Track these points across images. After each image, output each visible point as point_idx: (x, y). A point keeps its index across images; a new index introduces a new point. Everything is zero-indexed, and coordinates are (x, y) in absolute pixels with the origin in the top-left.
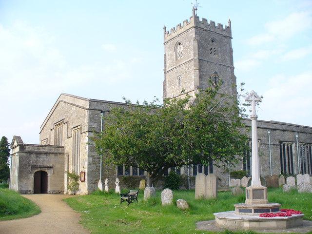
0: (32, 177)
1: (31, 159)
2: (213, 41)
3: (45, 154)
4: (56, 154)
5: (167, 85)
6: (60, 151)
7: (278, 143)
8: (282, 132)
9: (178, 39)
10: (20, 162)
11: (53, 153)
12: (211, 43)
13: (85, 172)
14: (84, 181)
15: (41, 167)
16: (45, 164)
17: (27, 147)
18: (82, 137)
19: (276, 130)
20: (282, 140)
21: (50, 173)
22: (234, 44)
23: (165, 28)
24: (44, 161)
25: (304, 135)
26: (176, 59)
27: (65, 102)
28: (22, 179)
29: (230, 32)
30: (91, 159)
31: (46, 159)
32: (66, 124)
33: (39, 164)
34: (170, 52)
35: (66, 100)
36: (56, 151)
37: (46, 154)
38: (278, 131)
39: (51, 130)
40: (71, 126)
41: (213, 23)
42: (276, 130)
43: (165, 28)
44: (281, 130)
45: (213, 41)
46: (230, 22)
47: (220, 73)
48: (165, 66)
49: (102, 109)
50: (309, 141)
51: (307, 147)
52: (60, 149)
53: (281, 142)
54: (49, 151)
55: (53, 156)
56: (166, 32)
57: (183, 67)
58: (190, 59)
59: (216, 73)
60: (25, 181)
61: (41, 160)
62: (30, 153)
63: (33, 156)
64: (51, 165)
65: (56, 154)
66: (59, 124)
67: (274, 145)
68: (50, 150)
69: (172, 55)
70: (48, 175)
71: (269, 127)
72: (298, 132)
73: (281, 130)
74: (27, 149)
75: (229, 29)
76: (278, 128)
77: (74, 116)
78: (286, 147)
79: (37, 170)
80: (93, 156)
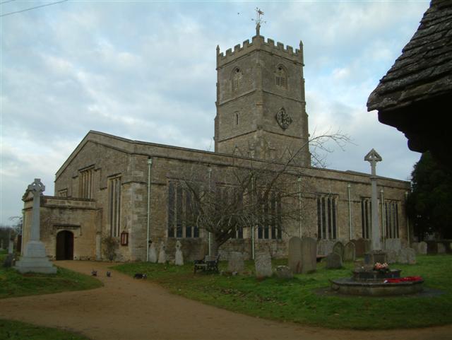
2: (280, 69)
4: (83, 209)
5: (220, 123)
7: (359, 199)
8: (365, 185)
9: (236, 64)
10: (42, 218)
11: (81, 209)
12: (278, 70)
13: (127, 234)
14: (127, 245)
16: (71, 222)
17: (48, 200)
18: (124, 188)
19: (357, 183)
20: (364, 196)
21: (76, 233)
22: (307, 73)
23: (218, 49)
24: (69, 218)
25: (390, 190)
26: (233, 90)
27: (96, 143)
29: (302, 57)
30: (136, 217)
31: (71, 216)
32: (98, 171)
33: (63, 223)
34: (225, 80)
35: (98, 140)
36: (84, 206)
37: (72, 209)
38: (360, 185)
39: (74, 178)
40: (106, 173)
41: (281, 45)
42: (357, 183)
43: (218, 49)
44: (363, 183)
45: (280, 69)
46: (301, 45)
47: (288, 109)
48: (218, 98)
49: (150, 153)
50: (395, 198)
51: (393, 205)
52: (90, 203)
53: (363, 198)
54: (76, 206)
55: (80, 212)
56: (219, 56)
57: (242, 100)
58: (252, 91)
59: (283, 109)
61: (65, 217)
62: (52, 208)
63: (56, 212)
64: (78, 224)
65: (83, 209)
66: (87, 171)
67: (354, 202)
68: (78, 204)
69: (226, 84)
70: (75, 236)
71: (349, 179)
72: (383, 186)
73: (363, 183)
74: (49, 203)
75: (300, 53)
76: (360, 181)
77: (111, 162)
78: (369, 204)
79: (60, 230)
80: (138, 213)
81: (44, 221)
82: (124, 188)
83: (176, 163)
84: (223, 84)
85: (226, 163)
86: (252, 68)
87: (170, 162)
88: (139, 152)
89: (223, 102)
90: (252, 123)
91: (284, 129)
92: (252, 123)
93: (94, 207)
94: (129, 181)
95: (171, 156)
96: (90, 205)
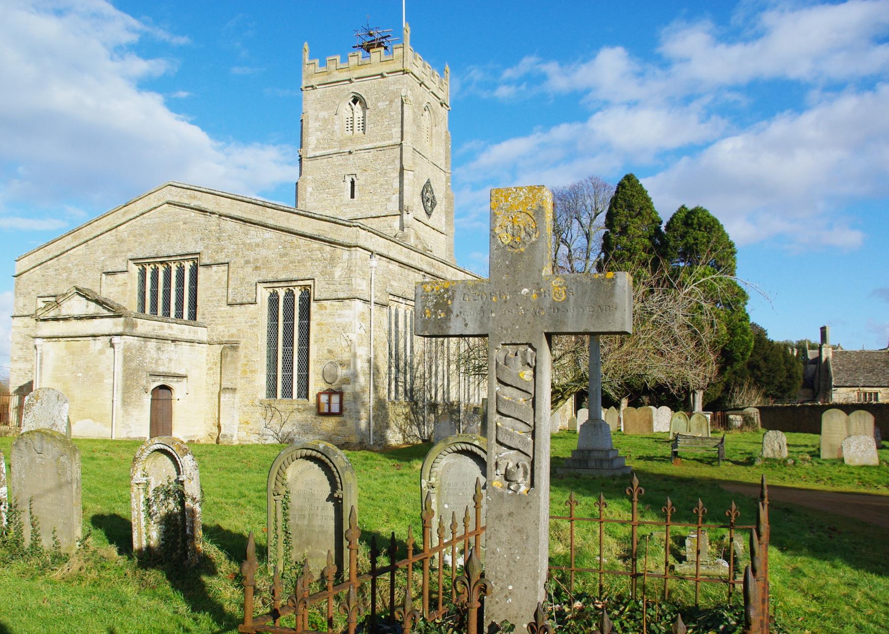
0: (147, 399)
1: (148, 355)
3: (173, 341)
5: (310, 189)
6: (199, 333)
10: (126, 360)
13: (341, 394)
15: (166, 376)
24: (170, 360)
28: (130, 408)
34: (323, 114)
35: (204, 206)
36: (191, 337)
39: (107, 273)
49: (371, 248)
54: (180, 336)
60: (135, 413)
61: (164, 356)
62: (146, 338)
63: (152, 344)
64: (182, 372)
69: (325, 120)
81: (133, 365)
82: (322, 307)
83: (394, 266)
84: (317, 119)
85: (439, 274)
86: (391, 102)
87: (391, 266)
88: (361, 243)
89: (318, 153)
90: (389, 200)
91: (429, 214)
92: (389, 200)
93: (205, 338)
94: (342, 296)
95: (391, 255)
96: (201, 334)
